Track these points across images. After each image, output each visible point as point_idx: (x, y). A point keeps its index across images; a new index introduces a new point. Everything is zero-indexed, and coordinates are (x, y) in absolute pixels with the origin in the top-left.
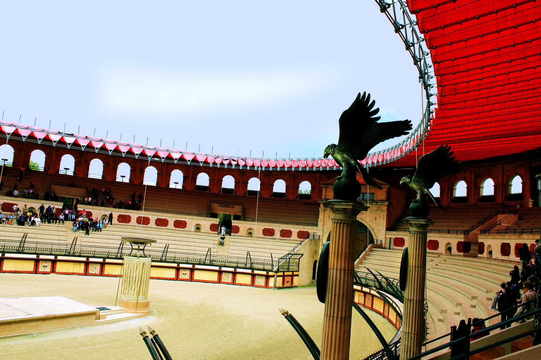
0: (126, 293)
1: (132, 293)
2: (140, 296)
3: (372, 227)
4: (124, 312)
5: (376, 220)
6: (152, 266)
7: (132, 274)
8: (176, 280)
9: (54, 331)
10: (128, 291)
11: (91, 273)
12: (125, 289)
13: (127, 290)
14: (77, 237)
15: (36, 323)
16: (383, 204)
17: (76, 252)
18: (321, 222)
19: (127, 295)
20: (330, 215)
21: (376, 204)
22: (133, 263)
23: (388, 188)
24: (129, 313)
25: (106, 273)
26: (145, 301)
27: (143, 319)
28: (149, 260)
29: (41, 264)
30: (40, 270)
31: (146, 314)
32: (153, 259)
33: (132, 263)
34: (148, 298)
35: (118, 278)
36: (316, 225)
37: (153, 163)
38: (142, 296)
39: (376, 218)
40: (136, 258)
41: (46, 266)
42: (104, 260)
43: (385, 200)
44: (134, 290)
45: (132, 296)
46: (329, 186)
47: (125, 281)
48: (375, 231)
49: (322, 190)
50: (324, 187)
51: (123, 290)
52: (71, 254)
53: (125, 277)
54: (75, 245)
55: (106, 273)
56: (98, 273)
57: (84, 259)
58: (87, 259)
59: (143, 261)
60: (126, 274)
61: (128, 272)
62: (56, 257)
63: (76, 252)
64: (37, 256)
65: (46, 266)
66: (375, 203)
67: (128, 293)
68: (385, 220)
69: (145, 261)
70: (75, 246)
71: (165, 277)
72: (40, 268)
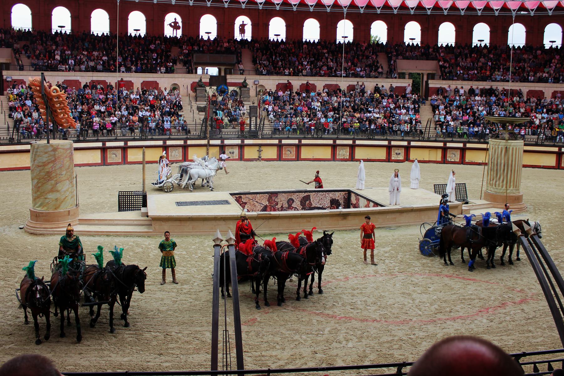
0: (492, 184)
1: (501, 184)
2: (510, 187)
4: (492, 207)
6: (525, 151)
7: (499, 161)
8: (556, 169)
9: (412, 225)
10: (496, 182)
11: (450, 160)
12: (491, 179)
13: (494, 181)
14: (431, 119)
15: (393, 216)
17: (431, 136)
19: (494, 186)
22: (500, 147)
24: (497, 208)
25: (467, 160)
26: (517, 194)
27: (515, 215)
28: (520, 144)
29: (394, 152)
30: (393, 158)
31: (519, 211)
32: (525, 142)
33: (498, 147)
34: (521, 190)
35: (482, 167)
37: (520, 19)
38: (513, 188)
40: (504, 141)
41: (399, 154)
42: (465, 145)
44: (503, 181)
45: (500, 188)
47: (491, 169)
51: (489, 180)
52: (426, 138)
53: (491, 165)
54: (430, 128)
55: (467, 160)
56: (458, 160)
57: (441, 144)
58: (445, 144)
59: (513, 144)
60: (493, 161)
61: (494, 159)
62: (409, 143)
63: (431, 136)
64: (388, 143)
65: (399, 154)
67: (495, 185)
69: (515, 144)
70: (429, 130)
71: (542, 164)
72: (392, 155)
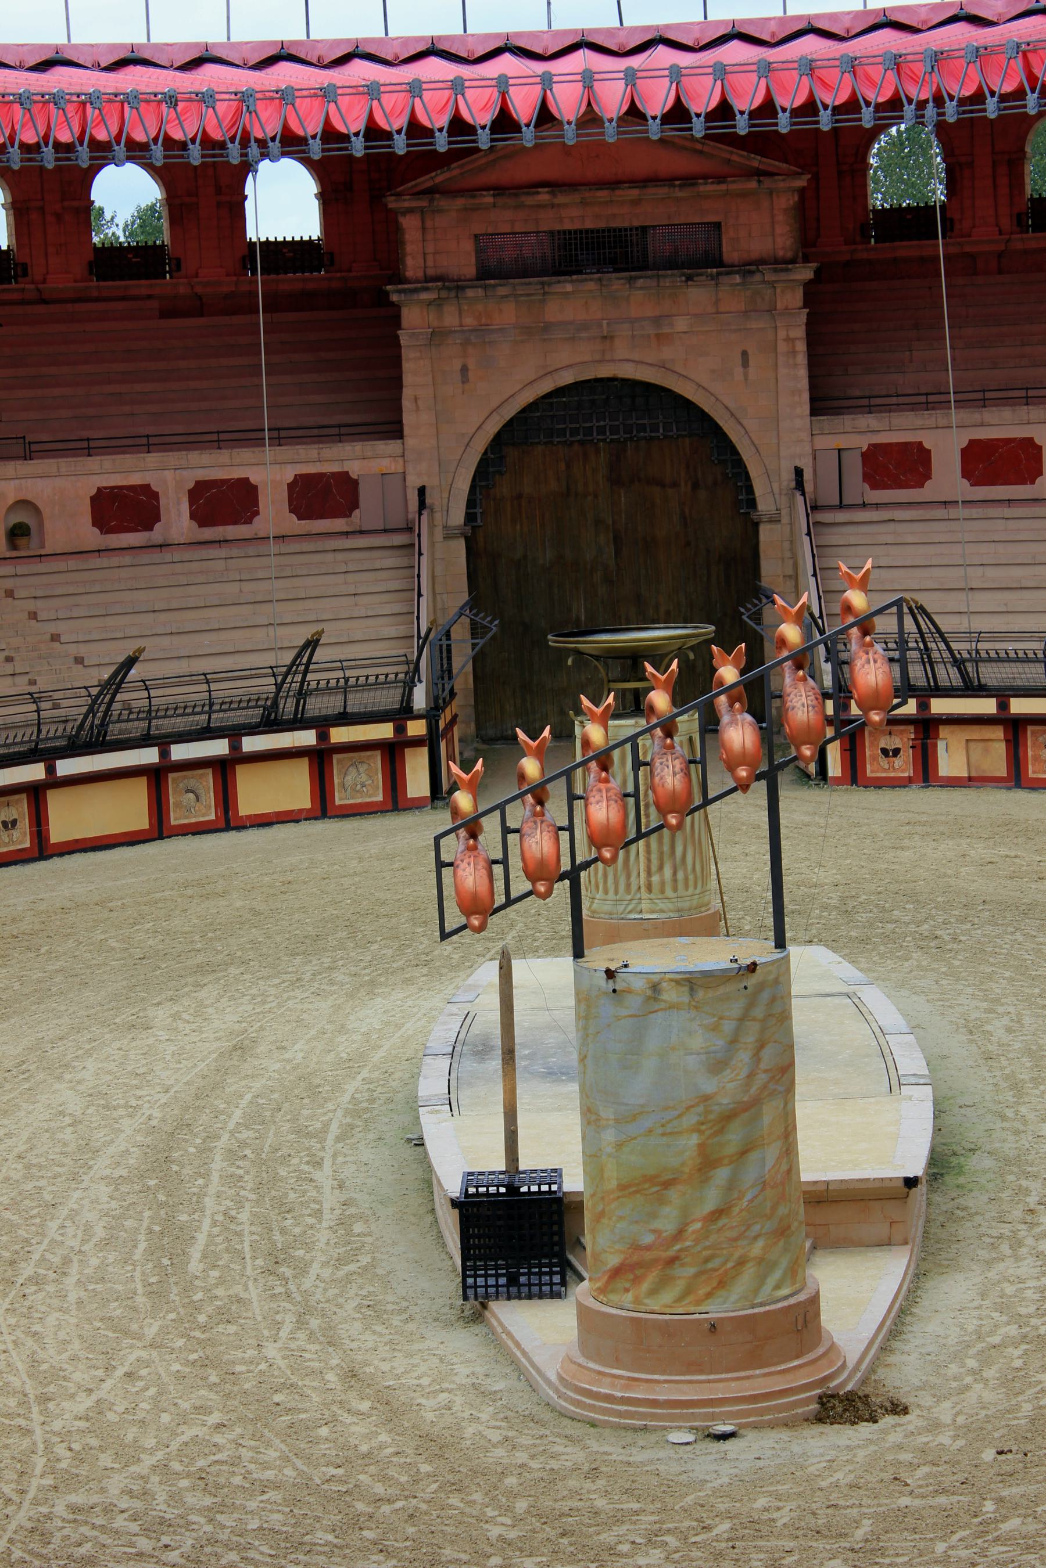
3: (731, 405)
5: (745, 363)
16: (783, 276)
18: (417, 409)
20: (471, 366)
21: (743, 284)
23: (802, 191)
36: (394, 430)
39: (745, 354)
43: (789, 255)
46: (443, 202)
48: (744, 422)
49: (398, 229)
50: (411, 211)
66: (738, 279)
68: (802, 359)
